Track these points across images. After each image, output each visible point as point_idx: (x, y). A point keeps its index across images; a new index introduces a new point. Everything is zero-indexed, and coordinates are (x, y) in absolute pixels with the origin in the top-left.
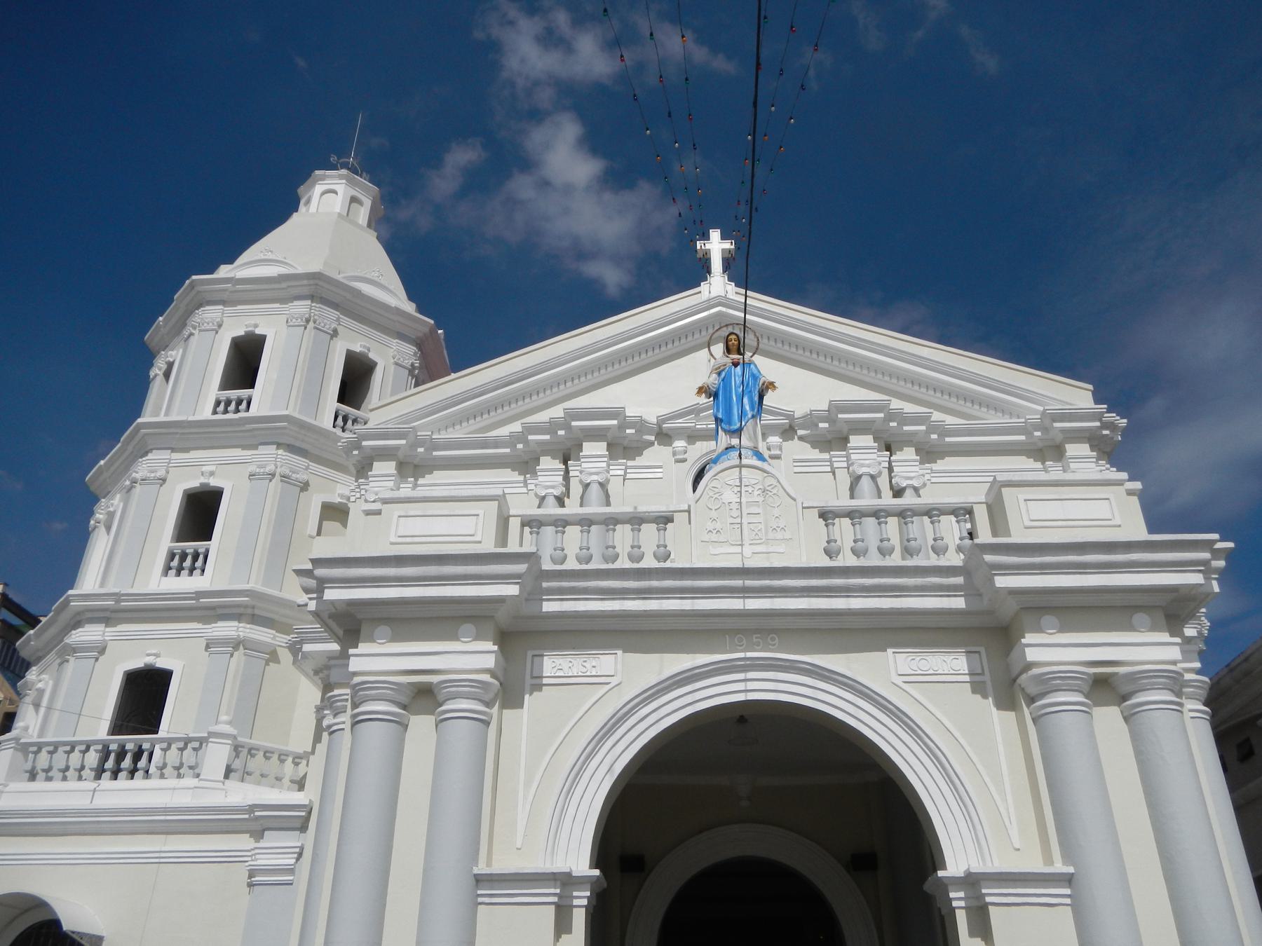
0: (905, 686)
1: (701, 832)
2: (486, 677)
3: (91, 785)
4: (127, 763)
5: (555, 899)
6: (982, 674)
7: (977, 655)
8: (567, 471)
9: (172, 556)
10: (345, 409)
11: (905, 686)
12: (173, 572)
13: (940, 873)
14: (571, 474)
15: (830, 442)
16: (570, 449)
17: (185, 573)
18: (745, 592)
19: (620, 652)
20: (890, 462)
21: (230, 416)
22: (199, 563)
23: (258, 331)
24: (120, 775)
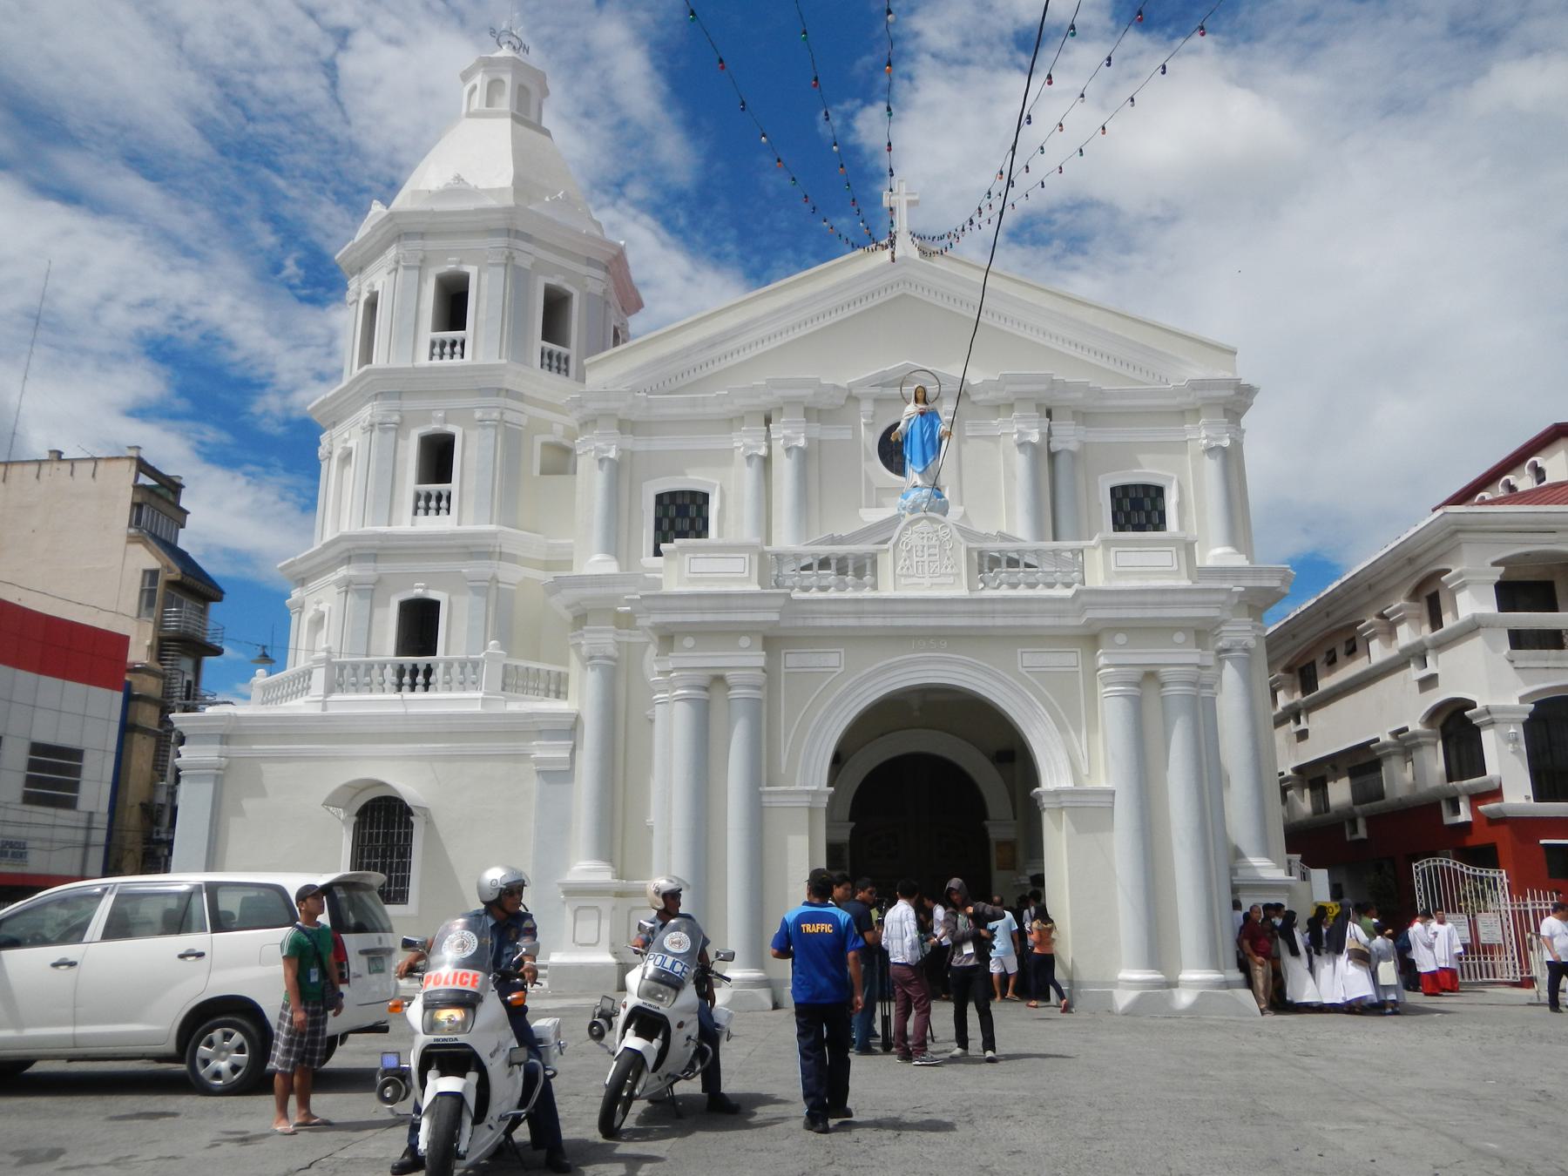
0: (1027, 675)
1: (882, 735)
2: (759, 672)
3: (397, 696)
4: (420, 679)
5: (809, 804)
6: (1077, 666)
8: (768, 430)
9: (418, 497)
10: (549, 346)
11: (1027, 675)
12: (421, 512)
13: (1037, 790)
14: (773, 436)
15: (998, 406)
16: (771, 411)
17: (432, 512)
18: (927, 614)
19: (842, 650)
20: (1049, 425)
21: (447, 361)
22: (444, 504)
24: (403, 688)
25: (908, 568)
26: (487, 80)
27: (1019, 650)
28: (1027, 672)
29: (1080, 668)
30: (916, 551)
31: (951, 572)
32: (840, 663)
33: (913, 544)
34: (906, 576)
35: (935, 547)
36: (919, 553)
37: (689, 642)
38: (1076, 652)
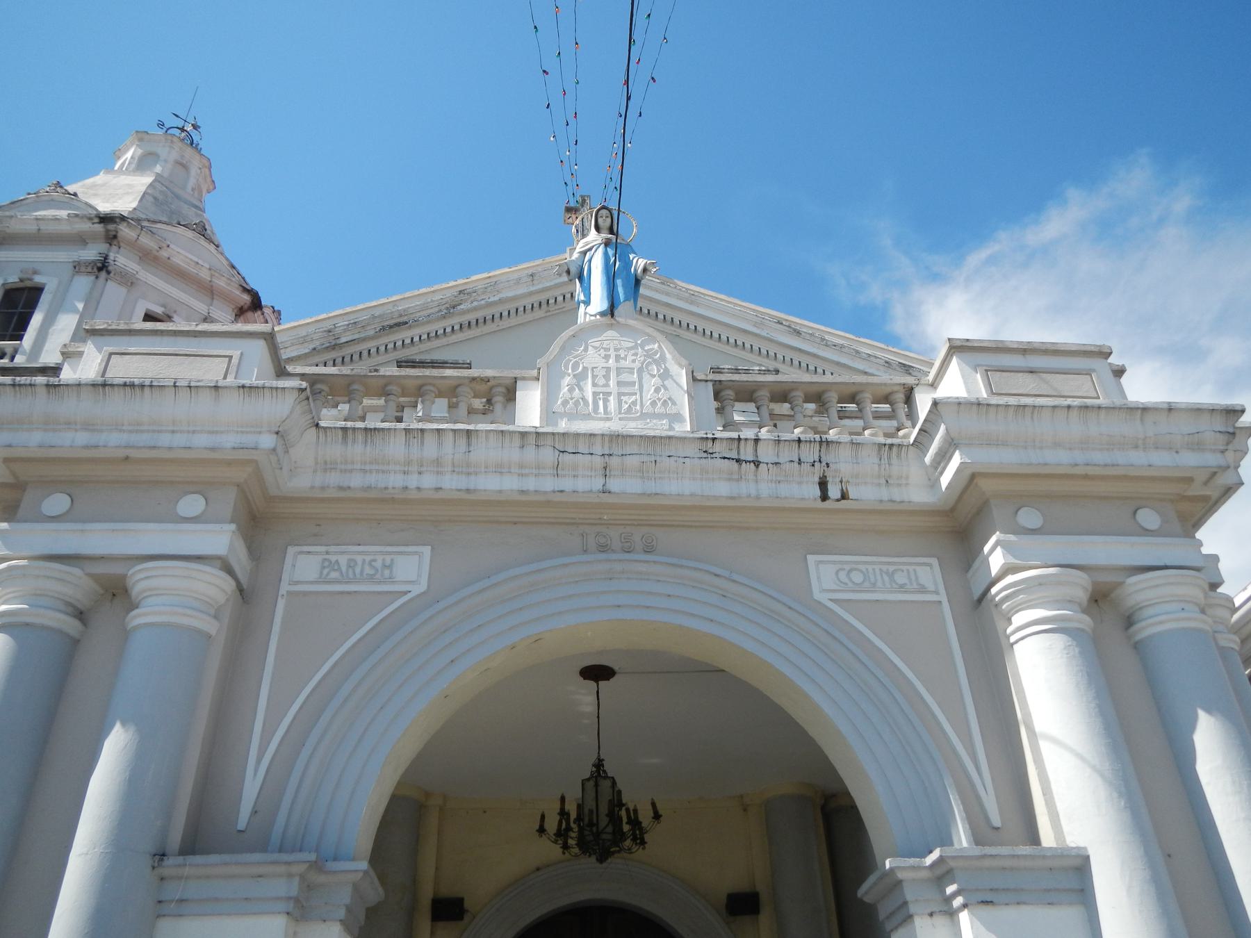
6: (937, 593)
7: (929, 568)
19: (427, 550)
23: (38, 279)
25: (577, 403)
26: (140, 151)
27: (811, 559)
28: (831, 600)
29: (944, 599)
30: (594, 377)
31: (662, 410)
32: (419, 575)
33: (590, 367)
34: (572, 417)
35: (631, 370)
36: (602, 381)
37: (57, 503)
38: (930, 565)
